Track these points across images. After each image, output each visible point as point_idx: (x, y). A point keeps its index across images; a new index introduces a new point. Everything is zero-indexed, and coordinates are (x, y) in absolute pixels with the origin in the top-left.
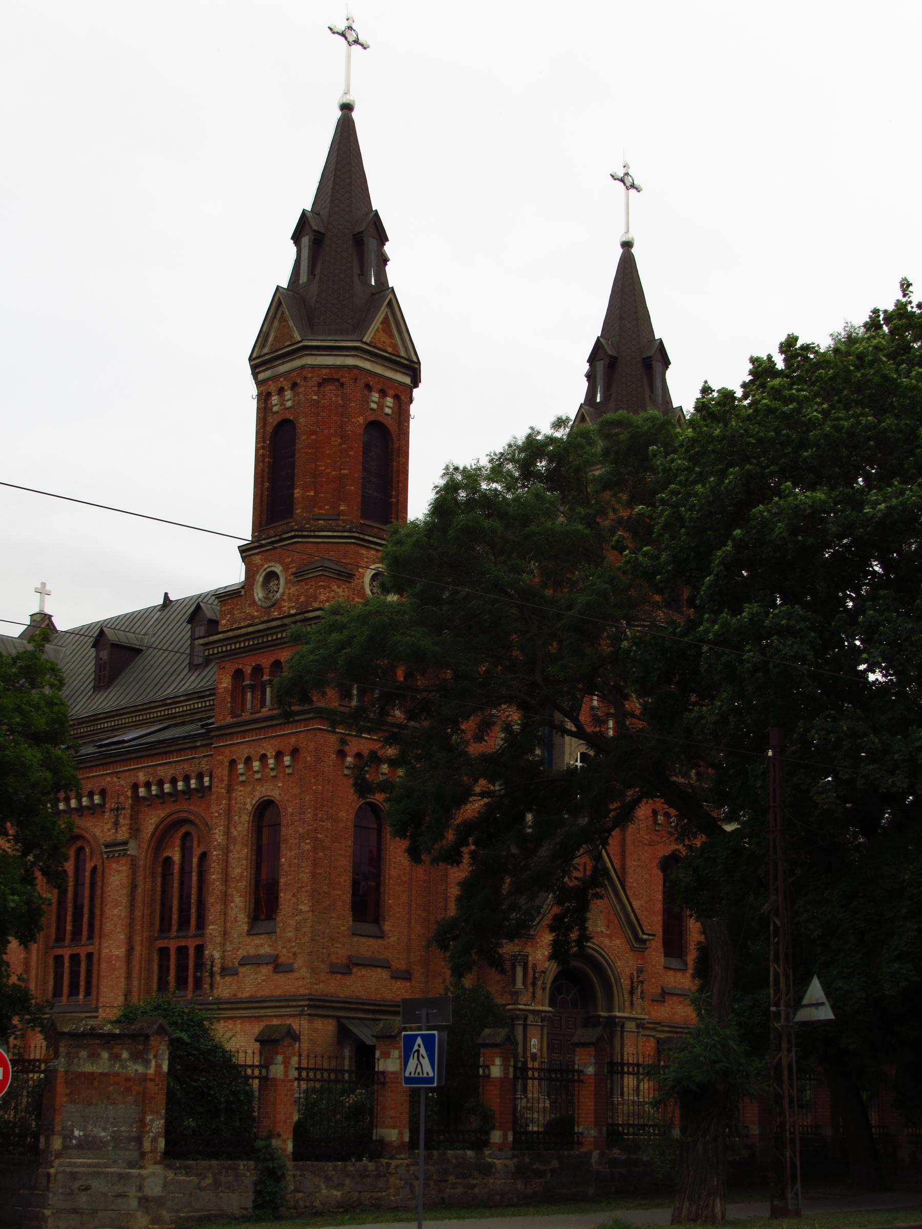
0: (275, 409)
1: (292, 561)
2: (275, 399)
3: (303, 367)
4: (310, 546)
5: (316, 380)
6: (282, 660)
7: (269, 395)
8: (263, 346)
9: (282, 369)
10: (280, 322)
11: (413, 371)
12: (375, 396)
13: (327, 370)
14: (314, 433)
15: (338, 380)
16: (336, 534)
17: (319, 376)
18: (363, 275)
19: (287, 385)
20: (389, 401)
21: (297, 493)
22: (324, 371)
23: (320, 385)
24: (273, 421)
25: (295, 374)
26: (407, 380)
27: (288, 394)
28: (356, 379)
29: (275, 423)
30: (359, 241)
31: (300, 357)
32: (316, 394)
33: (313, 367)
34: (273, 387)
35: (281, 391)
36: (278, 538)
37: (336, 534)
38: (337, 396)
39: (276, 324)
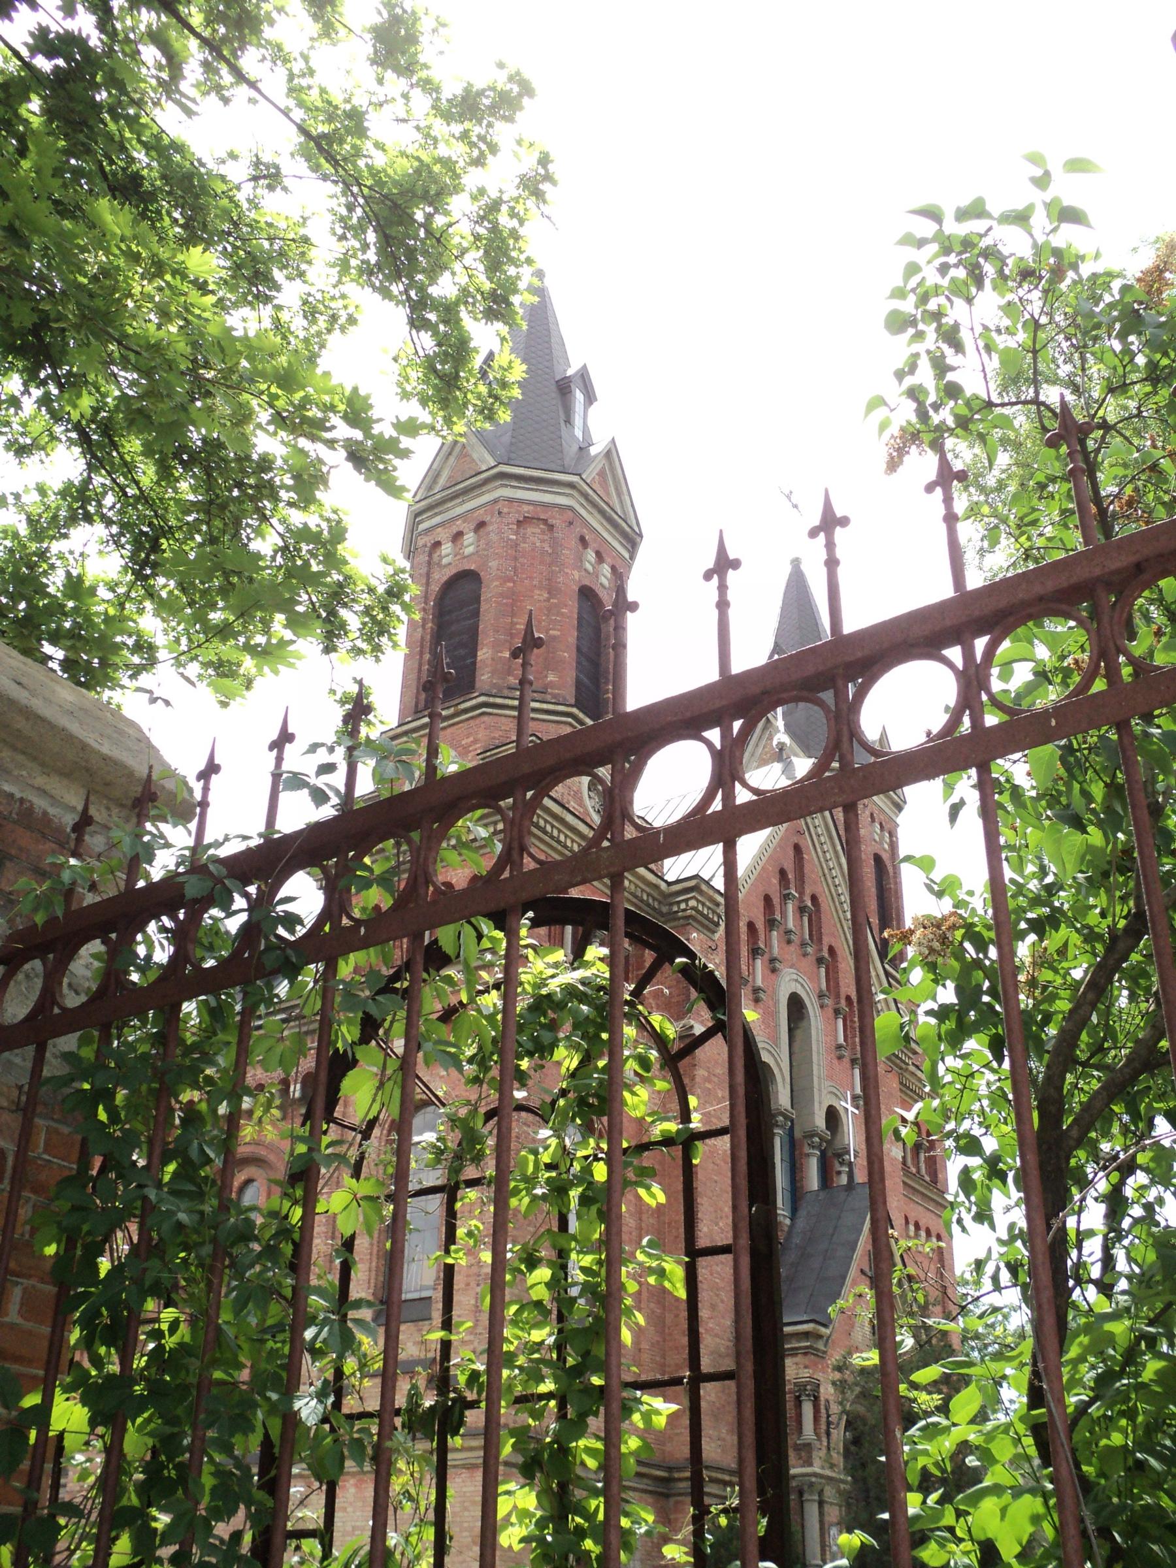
0: (445, 561)
1: (475, 741)
2: (447, 548)
3: (496, 501)
4: (503, 719)
5: (514, 517)
6: (454, 881)
7: (438, 544)
8: (430, 488)
9: (459, 510)
10: (458, 458)
11: (632, 540)
12: (591, 555)
13: (531, 508)
14: (510, 580)
15: (545, 521)
16: (545, 706)
17: (518, 512)
18: (568, 421)
19: (467, 527)
20: (606, 569)
21: (483, 654)
22: (526, 508)
23: (519, 523)
24: (441, 577)
25: (482, 511)
26: (627, 555)
27: (469, 538)
28: (571, 523)
29: (445, 578)
30: (564, 388)
31: (489, 491)
32: (517, 533)
33: (511, 501)
34: (443, 535)
35: (458, 535)
36: (452, 710)
37: (545, 706)
38: (543, 541)
39: (452, 459)
